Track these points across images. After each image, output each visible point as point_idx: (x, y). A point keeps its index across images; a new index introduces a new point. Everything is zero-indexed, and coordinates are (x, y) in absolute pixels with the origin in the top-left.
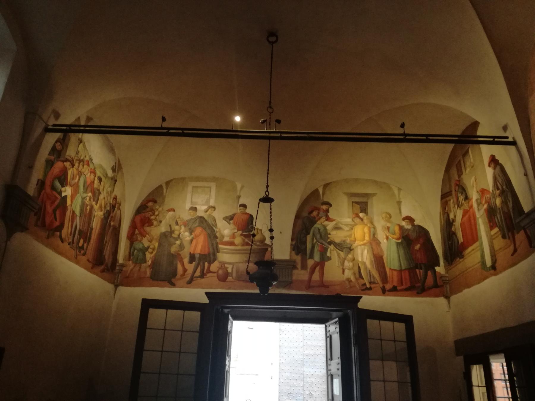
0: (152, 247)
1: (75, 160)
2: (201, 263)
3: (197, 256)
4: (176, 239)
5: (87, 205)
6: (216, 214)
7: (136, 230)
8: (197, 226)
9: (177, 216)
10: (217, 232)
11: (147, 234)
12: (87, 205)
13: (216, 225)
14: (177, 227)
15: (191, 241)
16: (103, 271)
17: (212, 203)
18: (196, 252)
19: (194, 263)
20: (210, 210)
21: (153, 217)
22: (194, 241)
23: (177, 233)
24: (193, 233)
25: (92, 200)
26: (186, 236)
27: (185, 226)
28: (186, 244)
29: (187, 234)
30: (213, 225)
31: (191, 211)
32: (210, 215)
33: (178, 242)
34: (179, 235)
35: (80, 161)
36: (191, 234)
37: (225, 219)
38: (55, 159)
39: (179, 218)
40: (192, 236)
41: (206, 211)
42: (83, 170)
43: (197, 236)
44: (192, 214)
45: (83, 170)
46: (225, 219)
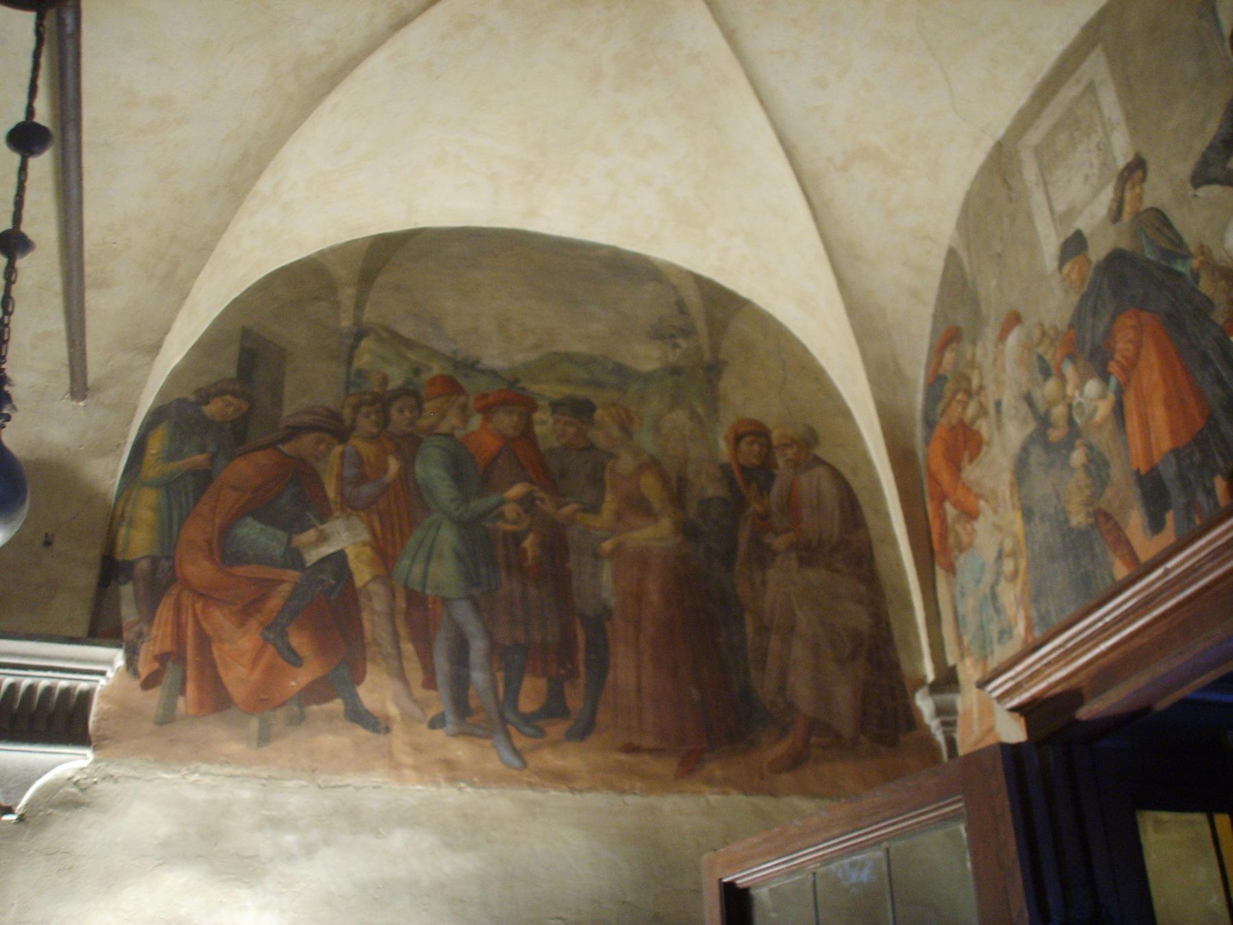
0: (1008, 545)
1: (347, 413)
2: (1201, 497)
3: (1169, 472)
4: (1068, 446)
5: (517, 538)
6: (1157, 191)
7: (948, 506)
8: (1113, 318)
9: (1036, 333)
10: (1196, 277)
11: (979, 496)
12: (517, 538)
13: (1176, 247)
14: (1051, 386)
15: (1119, 411)
16: (795, 761)
17: (1122, 150)
18: (1157, 459)
19: (1170, 517)
20: (1128, 196)
21: (971, 410)
22: (1130, 404)
23: (1059, 412)
24: (1113, 367)
25: (547, 507)
26: (1093, 397)
27: (1072, 357)
28: (1103, 439)
29: (1092, 387)
30: (1165, 254)
31: (1067, 268)
32: (1137, 215)
33: (1078, 457)
34: (1071, 421)
35: (383, 402)
36: (1105, 376)
37: (1200, 178)
38: (213, 458)
39: (1044, 334)
40: (1113, 381)
41: (1116, 214)
42: (424, 423)
43: (1130, 367)
44: (1074, 276)
45: (424, 423)
46: (1200, 178)
